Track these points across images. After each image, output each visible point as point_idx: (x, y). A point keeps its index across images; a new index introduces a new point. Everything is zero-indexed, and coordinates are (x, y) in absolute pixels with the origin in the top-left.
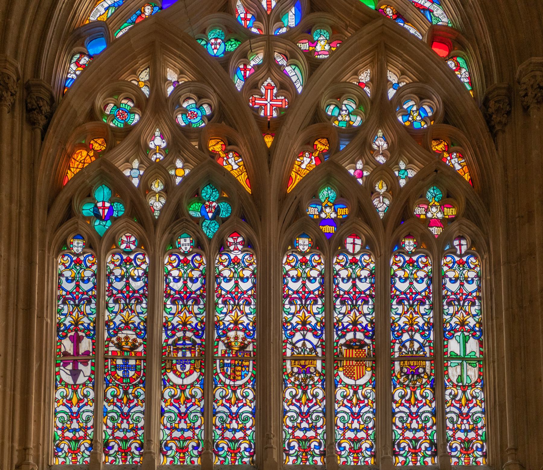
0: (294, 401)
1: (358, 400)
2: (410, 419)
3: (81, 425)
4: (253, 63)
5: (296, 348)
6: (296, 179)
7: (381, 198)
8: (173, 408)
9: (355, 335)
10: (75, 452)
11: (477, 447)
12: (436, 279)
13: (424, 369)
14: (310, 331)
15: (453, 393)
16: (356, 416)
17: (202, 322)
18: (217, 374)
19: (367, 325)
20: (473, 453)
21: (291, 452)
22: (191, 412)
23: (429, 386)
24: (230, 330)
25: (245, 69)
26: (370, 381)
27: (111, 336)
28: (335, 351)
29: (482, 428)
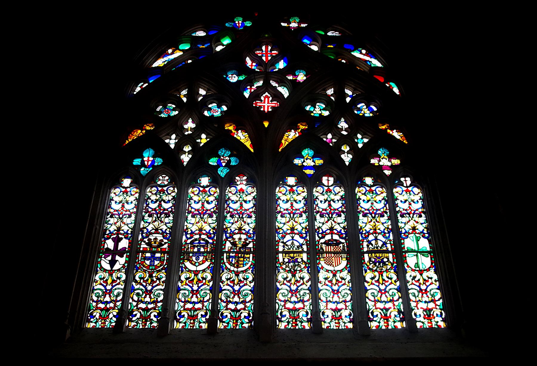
0: (285, 282)
1: (337, 280)
2: (380, 294)
3: (112, 299)
4: (256, 86)
5: (287, 245)
6: (285, 143)
7: (346, 154)
8: (187, 287)
9: (332, 236)
10: (104, 318)
11: (437, 315)
12: (391, 201)
13: (388, 259)
14: (297, 234)
15: (413, 276)
16: (336, 292)
17: (214, 228)
18: (224, 263)
19: (341, 230)
20: (434, 318)
21: (283, 319)
22: (202, 290)
23: (392, 271)
24: (235, 234)
25: (251, 88)
26: (346, 267)
27: (143, 238)
28: (317, 247)
29: (439, 300)
